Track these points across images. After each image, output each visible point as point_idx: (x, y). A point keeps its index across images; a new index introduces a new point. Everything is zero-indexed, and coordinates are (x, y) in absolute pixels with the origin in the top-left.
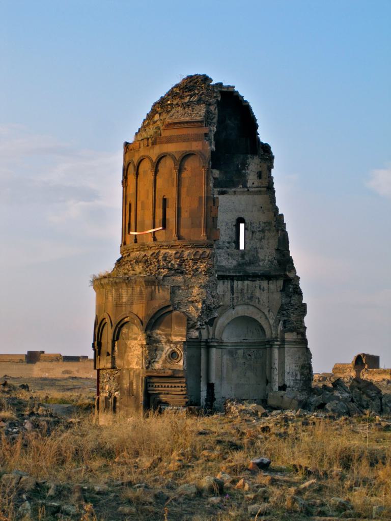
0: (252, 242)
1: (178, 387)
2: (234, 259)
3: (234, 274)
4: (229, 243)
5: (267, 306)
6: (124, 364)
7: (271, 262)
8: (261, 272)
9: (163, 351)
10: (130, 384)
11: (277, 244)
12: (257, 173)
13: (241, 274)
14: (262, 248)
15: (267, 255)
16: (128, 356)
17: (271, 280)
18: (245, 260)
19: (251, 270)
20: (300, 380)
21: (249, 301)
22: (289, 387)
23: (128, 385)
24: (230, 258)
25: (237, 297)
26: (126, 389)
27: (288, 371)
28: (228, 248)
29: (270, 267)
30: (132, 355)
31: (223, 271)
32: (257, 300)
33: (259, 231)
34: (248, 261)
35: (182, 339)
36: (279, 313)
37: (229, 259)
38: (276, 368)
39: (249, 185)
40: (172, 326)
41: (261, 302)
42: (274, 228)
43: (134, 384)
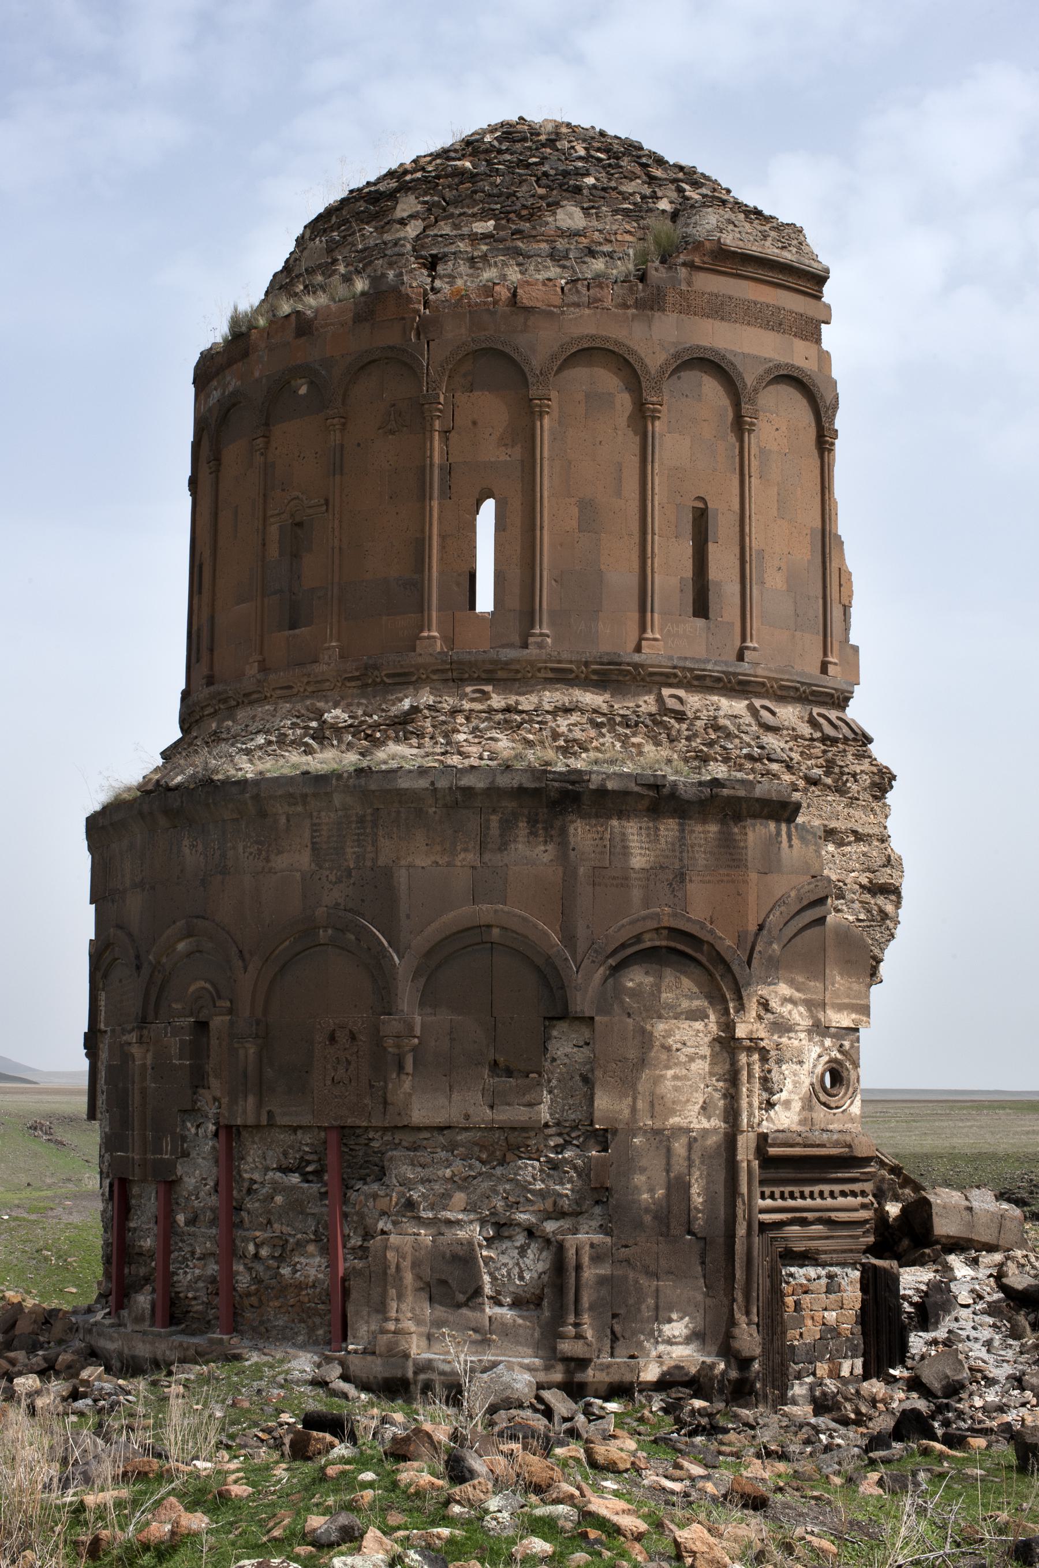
6: (634, 1109)
9: (801, 1063)
10: (669, 1188)
16: (658, 1080)
23: (660, 1192)
26: (647, 1210)
30: (676, 1077)
40: (827, 971)
43: (695, 1189)
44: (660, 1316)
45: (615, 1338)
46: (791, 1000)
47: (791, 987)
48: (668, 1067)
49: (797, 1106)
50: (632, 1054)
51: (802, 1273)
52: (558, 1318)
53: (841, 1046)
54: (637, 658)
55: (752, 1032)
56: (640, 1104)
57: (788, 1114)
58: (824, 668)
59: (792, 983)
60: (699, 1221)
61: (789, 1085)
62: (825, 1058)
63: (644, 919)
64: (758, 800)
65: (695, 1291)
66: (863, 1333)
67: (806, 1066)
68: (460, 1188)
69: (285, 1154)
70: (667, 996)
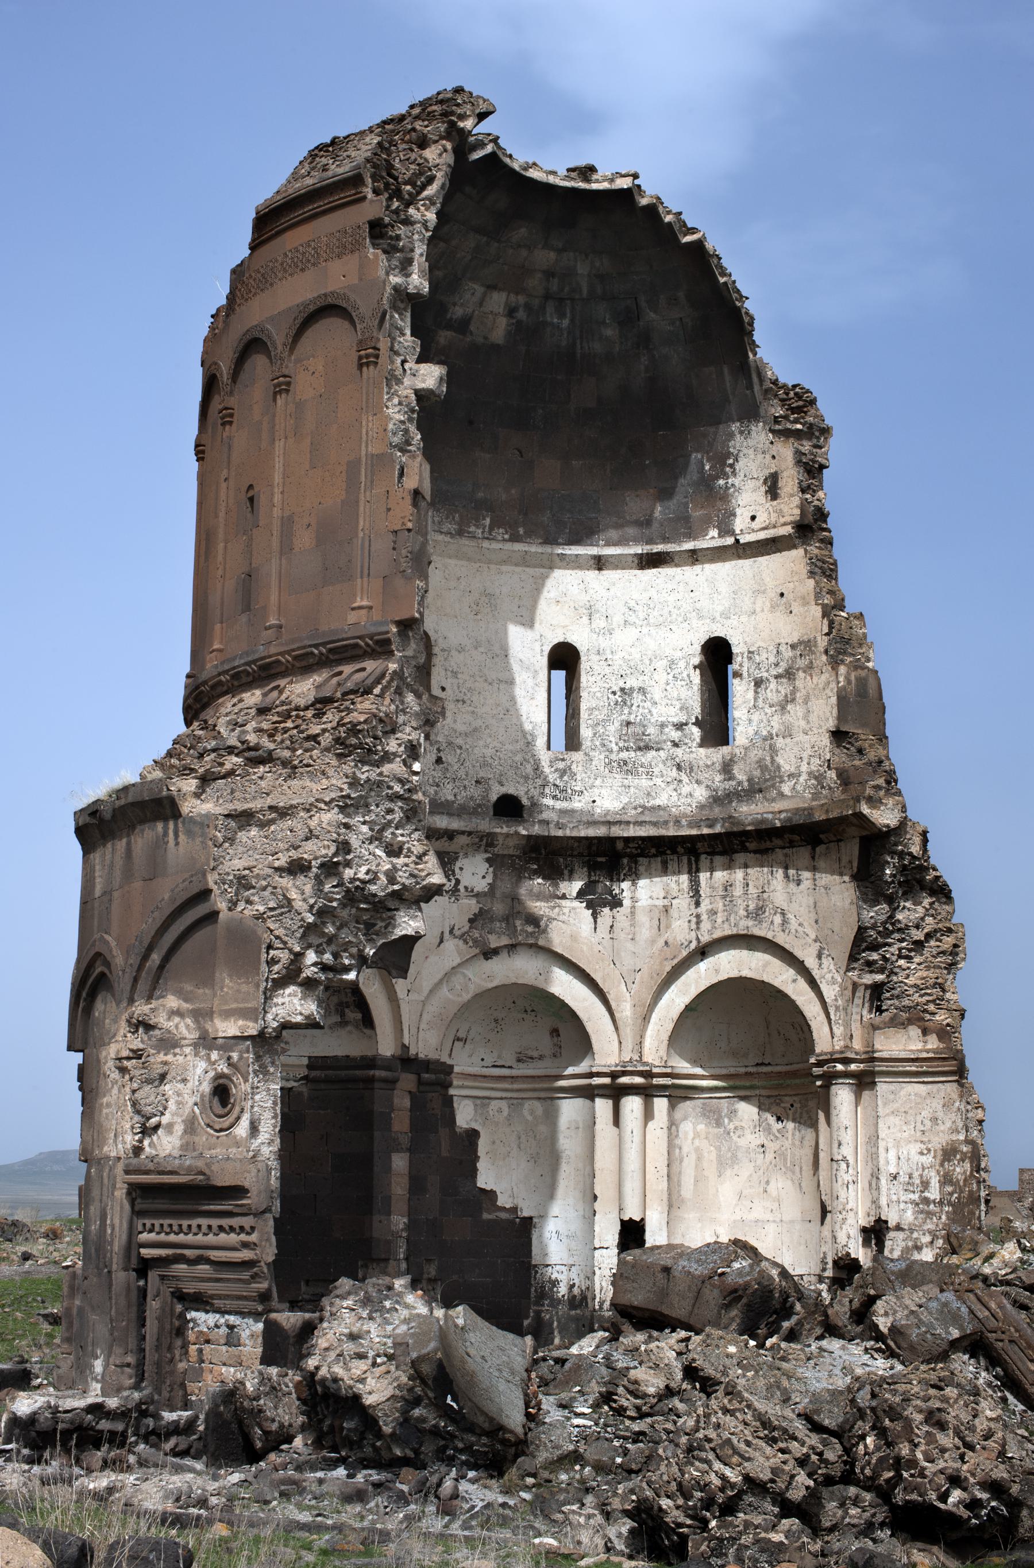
0: (756, 717)
1: (232, 1229)
2: (698, 782)
3: (694, 832)
4: (680, 726)
5: (813, 937)
7: (819, 778)
8: (783, 815)
9: (184, 1081)
11: (835, 711)
12: (765, 482)
13: (718, 829)
14: (787, 733)
15: (805, 755)
17: (820, 842)
18: (734, 783)
19: (751, 812)
20: (941, 1203)
21: (750, 923)
22: (898, 1228)
24: (685, 779)
25: (713, 913)
27: (893, 1170)
28: (676, 745)
29: (815, 796)
31: (655, 824)
32: (778, 919)
33: (776, 677)
34: (746, 784)
35: (242, 1029)
36: (853, 958)
37: (680, 781)
38: (844, 1159)
39: (740, 523)
41: (793, 924)
42: (824, 658)
46: (178, 1013)
47: (179, 998)
49: (179, 1129)
51: (203, 1320)
53: (229, 1058)
55: (118, 1052)
57: (170, 1139)
61: (172, 1105)
62: (212, 1074)
64: (133, 804)
67: (190, 1085)
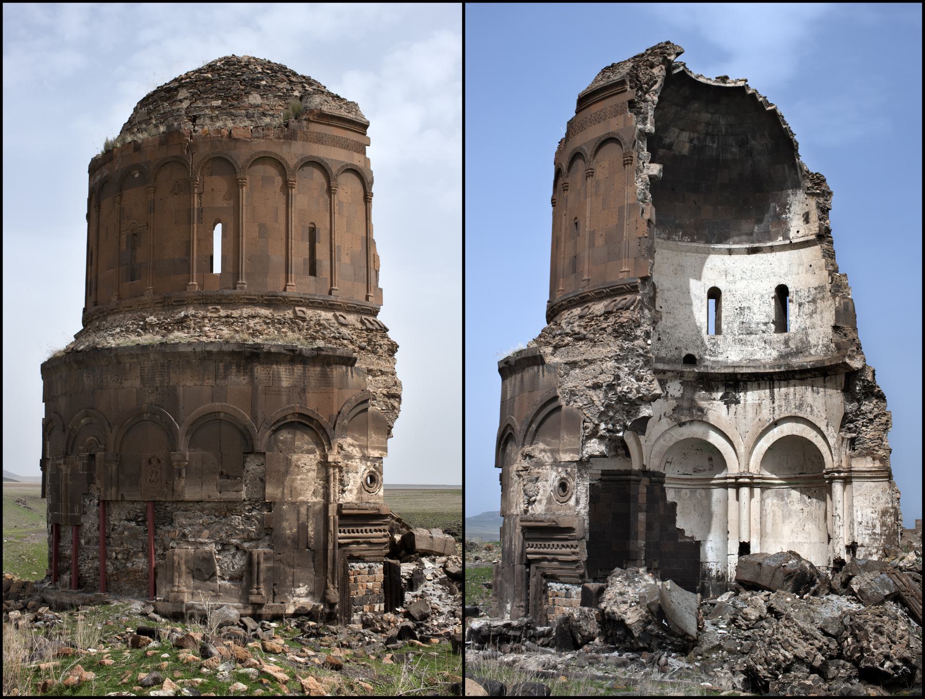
6: (283, 493)
9: (357, 473)
10: (298, 528)
16: (294, 480)
23: (295, 530)
26: (289, 538)
30: (302, 479)
43: (310, 529)
44: (295, 585)
45: (274, 594)
48: (298, 475)
49: (355, 492)
50: (282, 469)
51: (357, 566)
52: (250, 586)
54: (284, 294)
56: (286, 491)
58: (367, 298)
59: (353, 437)
60: (312, 543)
61: (352, 483)
63: (288, 409)
65: (310, 574)
66: (385, 592)
68: (206, 528)
69: (129, 513)
70: (297, 443)
